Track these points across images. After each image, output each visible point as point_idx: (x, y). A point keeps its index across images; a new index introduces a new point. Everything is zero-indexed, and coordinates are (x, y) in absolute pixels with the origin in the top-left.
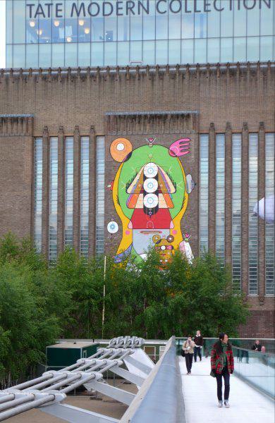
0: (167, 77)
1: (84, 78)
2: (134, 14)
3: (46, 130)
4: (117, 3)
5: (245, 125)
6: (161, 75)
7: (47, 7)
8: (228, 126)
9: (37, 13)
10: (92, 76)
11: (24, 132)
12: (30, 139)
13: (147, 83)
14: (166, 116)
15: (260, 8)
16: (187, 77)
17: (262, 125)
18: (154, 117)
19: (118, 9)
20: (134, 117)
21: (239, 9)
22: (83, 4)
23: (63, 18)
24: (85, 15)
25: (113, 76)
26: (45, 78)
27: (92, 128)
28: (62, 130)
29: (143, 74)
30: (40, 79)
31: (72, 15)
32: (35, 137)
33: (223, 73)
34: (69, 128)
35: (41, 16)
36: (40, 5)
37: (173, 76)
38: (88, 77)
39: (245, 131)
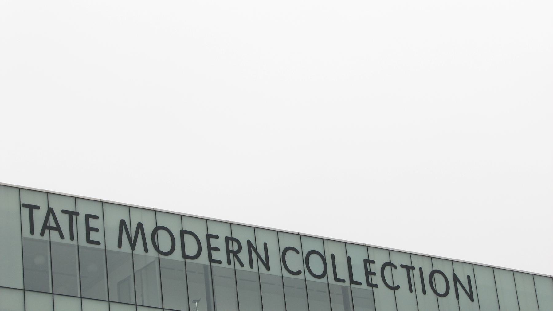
2: (242, 265)
4: (209, 237)
7: (66, 216)
9: (46, 227)
15: (458, 298)
19: (210, 249)
21: (424, 292)
22: (140, 226)
23: (102, 246)
24: (146, 250)
31: (120, 246)
35: (55, 235)
36: (50, 211)
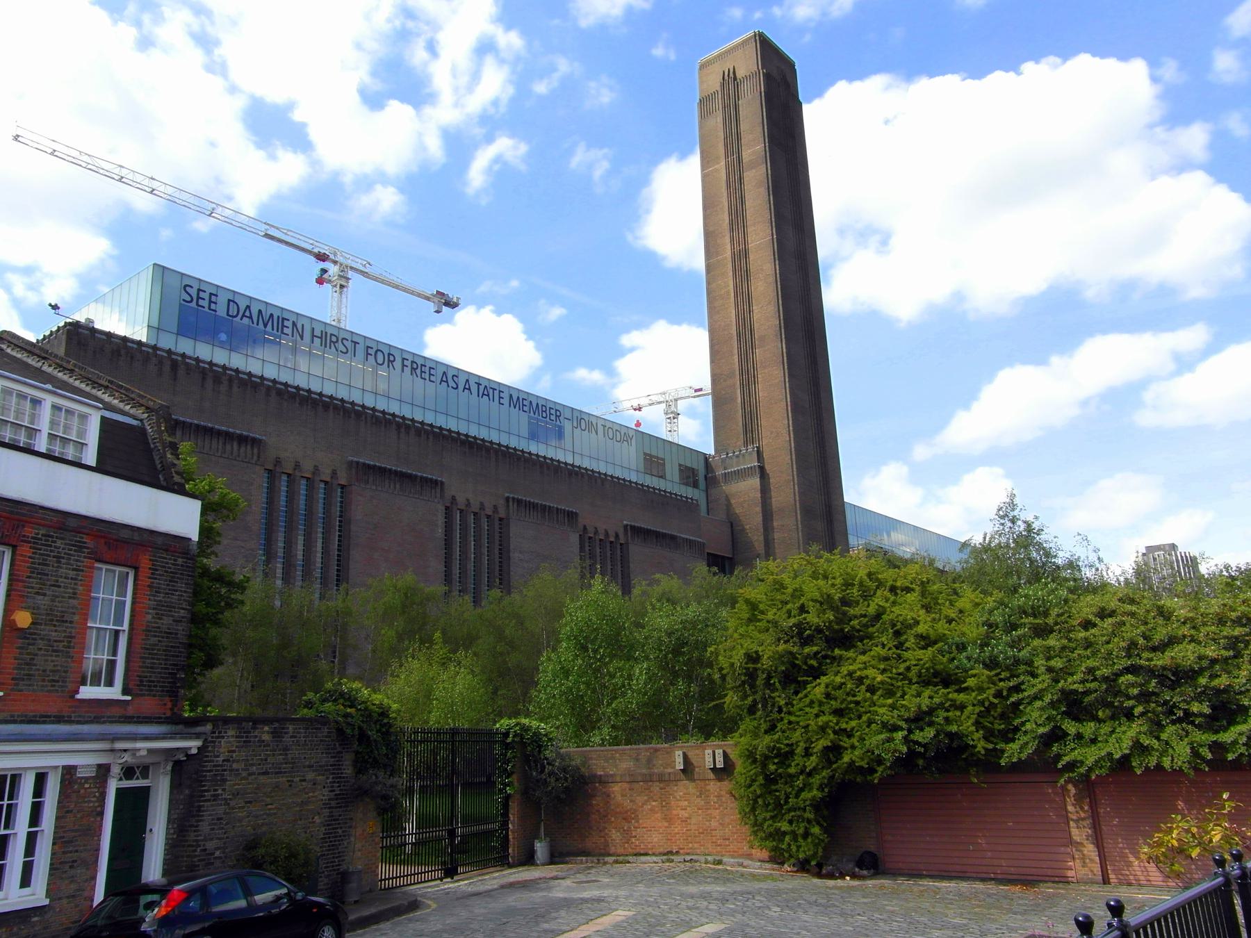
0: (412, 432)
1: (326, 406)
3: (278, 462)
11: (255, 458)
14: (416, 476)
20: (382, 471)
26: (280, 393)
30: (273, 393)
33: (463, 443)
34: (307, 467)
38: (331, 407)
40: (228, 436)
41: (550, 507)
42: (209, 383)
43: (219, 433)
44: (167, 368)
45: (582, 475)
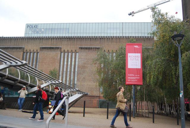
1: (36, 39)
3: (27, 50)
5: (72, 50)
6: (54, 38)
8: (68, 50)
10: (38, 38)
12: (22, 52)
13: (50, 40)
14: (54, 47)
16: (59, 39)
17: (76, 50)
18: (50, 48)
25: (43, 39)
26: (28, 39)
27: (37, 50)
28: (30, 50)
29: (50, 38)
30: (27, 39)
32: (24, 52)
33: (68, 38)
37: (56, 39)
39: (72, 52)
40: (17, 48)
41: (91, 48)
42: (16, 40)
43: (16, 48)
44: (10, 40)
45: (105, 38)
